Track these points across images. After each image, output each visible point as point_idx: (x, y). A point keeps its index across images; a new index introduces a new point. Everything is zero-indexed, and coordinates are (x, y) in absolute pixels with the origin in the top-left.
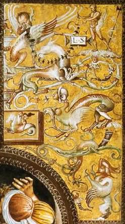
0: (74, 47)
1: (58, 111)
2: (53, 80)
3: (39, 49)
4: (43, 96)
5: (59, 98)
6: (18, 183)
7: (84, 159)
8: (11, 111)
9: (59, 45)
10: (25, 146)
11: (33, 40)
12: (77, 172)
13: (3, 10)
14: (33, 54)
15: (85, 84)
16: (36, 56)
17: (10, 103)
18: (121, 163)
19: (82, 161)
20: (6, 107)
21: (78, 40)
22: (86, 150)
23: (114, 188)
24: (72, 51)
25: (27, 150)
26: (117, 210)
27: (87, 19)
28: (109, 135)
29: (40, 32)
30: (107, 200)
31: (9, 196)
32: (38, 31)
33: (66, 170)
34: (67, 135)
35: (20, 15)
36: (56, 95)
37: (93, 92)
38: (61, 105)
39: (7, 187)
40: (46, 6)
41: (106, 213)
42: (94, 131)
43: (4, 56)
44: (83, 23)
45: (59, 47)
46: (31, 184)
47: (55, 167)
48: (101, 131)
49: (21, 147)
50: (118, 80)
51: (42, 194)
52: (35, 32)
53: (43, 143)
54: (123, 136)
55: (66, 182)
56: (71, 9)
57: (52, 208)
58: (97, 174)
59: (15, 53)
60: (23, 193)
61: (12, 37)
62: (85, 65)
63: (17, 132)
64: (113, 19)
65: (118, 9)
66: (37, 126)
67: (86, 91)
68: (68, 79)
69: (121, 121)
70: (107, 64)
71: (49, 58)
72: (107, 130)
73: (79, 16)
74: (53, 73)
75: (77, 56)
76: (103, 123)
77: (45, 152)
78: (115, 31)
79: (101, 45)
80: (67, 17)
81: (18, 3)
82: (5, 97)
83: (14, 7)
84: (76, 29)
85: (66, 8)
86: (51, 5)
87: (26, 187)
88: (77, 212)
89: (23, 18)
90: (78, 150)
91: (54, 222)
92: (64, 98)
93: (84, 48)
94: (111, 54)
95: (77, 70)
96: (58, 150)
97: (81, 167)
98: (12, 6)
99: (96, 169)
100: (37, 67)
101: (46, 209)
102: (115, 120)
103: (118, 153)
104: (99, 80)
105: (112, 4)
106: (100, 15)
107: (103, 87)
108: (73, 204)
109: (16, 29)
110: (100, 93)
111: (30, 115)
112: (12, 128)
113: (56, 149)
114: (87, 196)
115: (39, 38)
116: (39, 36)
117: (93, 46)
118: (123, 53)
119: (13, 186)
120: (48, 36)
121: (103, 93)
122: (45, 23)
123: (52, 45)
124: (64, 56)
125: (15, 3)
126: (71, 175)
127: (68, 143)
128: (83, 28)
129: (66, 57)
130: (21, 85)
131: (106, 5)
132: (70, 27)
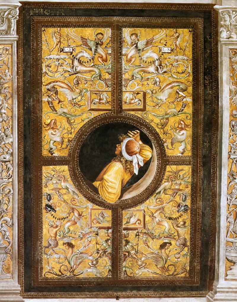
1: (154, 91)
2: (152, 73)
3: (143, 55)
4: (145, 83)
5: (155, 84)
6: (131, 134)
7: (169, 119)
8: (127, 92)
9: (155, 53)
10: (135, 112)
11: (140, 50)
12: (165, 127)
13: (122, 32)
14: (140, 58)
15: (171, 75)
16: (141, 59)
17: (126, 87)
18: (191, 122)
19: (168, 121)
20: (124, 89)
21: (166, 50)
22: (171, 114)
23: (187, 136)
24: (162, 56)
25: (136, 114)
26: (189, 149)
27: (172, 38)
28: (185, 105)
29: (144, 45)
30: (183, 144)
32: (143, 44)
33: (159, 126)
34: (159, 105)
35: (132, 35)
36: (153, 82)
37: (175, 80)
38: (156, 88)
39: (125, 136)
40: (148, 30)
41: (183, 151)
42: (175, 103)
43: (123, 59)
44: (169, 40)
45: (154, 53)
46: (139, 134)
47: (153, 124)
48: (180, 103)
49: (132, 113)
50: (190, 73)
51: (145, 140)
52: (141, 45)
53: (145, 110)
54: (193, 106)
55: (159, 133)
56: (162, 31)
58: (177, 128)
59: (129, 57)
61: (128, 48)
62: (170, 64)
63: (130, 103)
64: (187, 38)
65: (189, 31)
66: (142, 100)
67: (171, 79)
68: (160, 72)
69: (191, 97)
70: (183, 63)
71: (149, 60)
72: (183, 103)
73: (166, 35)
74: (152, 69)
75: (166, 59)
76: (181, 98)
77: (147, 116)
78: (188, 44)
79: (180, 53)
80: (160, 36)
81: (131, 28)
82: (123, 83)
83: (129, 30)
84: (165, 43)
85: (159, 31)
86: (150, 29)
87: (136, 136)
88: (165, 150)
89: (134, 37)
90: (166, 114)
91: (152, 156)
92: (158, 84)
93: (170, 54)
94: (186, 58)
95: (165, 67)
96: (154, 114)
98: (127, 29)
99: (177, 125)
100: (142, 66)
101: (148, 149)
102: (188, 96)
103: (190, 116)
104: (179, 73)
105: (186, 28)
106: (179, 35)
107: (181, 77)
108: (163, 146)
109: (130, 43)
110: (179, 80)
111: (138, 94)
112: (128, 101)
113: (153, 114)
115: (143, 48)
116: (144, 47)
117: (175, 53)
118: (193, 57)
119: (128, 135)
120: (148, 47)
121: (181, 81)
122: (147, 40)
123: (150, 53)
124: (158, 59)
125: (129, 28)
126: (162, 129)
127: (160, 110)
128: (169, 43)
129: (159, 59)
130: (133, 76)
131: (183, 29)
132: (161, 42)
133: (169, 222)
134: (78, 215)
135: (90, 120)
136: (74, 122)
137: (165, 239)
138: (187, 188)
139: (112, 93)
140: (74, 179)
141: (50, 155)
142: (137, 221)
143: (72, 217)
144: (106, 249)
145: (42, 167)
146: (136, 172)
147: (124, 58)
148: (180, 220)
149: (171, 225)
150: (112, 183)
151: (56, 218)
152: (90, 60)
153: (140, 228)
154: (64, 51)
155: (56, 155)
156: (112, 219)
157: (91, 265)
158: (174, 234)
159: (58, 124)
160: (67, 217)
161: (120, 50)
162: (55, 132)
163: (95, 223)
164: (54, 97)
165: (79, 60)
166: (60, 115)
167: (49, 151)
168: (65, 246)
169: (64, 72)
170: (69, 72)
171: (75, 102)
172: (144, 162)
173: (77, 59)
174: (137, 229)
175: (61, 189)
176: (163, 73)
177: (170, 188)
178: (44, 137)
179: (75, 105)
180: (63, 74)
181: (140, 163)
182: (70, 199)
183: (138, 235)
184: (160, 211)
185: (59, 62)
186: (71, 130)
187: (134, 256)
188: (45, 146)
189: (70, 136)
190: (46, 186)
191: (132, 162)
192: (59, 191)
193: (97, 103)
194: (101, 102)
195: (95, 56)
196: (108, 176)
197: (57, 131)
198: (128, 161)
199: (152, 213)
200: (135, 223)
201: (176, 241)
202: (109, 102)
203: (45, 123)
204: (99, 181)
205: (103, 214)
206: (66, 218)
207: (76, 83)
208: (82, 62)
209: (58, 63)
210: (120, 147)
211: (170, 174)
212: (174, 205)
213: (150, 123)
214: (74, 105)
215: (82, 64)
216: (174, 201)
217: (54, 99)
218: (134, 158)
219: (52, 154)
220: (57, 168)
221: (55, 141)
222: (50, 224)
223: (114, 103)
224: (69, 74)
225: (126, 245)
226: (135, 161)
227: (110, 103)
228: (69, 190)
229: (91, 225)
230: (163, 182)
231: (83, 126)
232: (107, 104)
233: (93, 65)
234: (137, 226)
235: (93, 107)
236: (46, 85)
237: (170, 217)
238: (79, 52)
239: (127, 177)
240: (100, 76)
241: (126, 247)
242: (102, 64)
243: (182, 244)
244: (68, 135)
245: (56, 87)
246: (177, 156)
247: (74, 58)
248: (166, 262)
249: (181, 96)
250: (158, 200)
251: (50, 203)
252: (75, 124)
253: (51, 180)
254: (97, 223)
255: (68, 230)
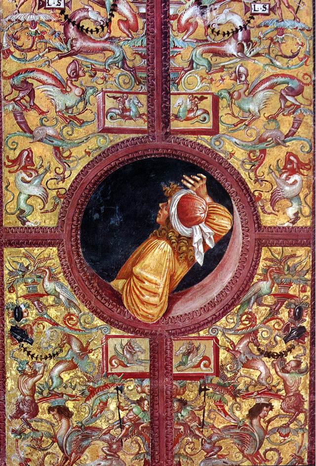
0: (255, 17)
1: (236, 94)
4: (217, 76)
5: (237, 78)
6: (188, 181)
7: (267, 152)
8: (179, 94)
10: (196, 136)
12: (259, 168)
15: (268, 61)
17: (178, 84)
20: (173, 90)
22: (269, 141)
24: (252, 21)
25: (199, 141)
26: (307, 214)
31: (177, 197)
33: (247, 165)
37: (278, 71)
39: (175, 186)
41: (294, 217)
45: (237, 15)
46: (205, 182)
49: (192, 138)
51: (218, 194)
53: (218, 133)
55: (247, 180)
57: (231, 213)
58: (284, 171)
59: (183, 21)
60: (195, 193)
63: (188, 119)
68: (248, 55)
74: (231, 48)
76: (290, 109)
77: (220, 143)
82: (172, 76)
87: (198, 186)
88: (259, 216)
91: (232, 228)
92: (243, 79)
96: (237, 141)
97: (264, 162)
99: (282, 164)
104: (286, 57)
110: (286, 72)
111: (202, 99)
112: (181, 114)
113: (234, 140)
114: (271, 197)
119: (182, 184)
124: (242, 26)
126: (252, 171)
129: (246, 29)
130: (192, 62)
133: (267, 362)
134: (80, 350)
135: (104, 153)
136: (69, 157)
137: (259, 396)
138: (305, 291)
139: (149, 97)
140: (71, 275)
141: (20, 224)
142: (201, 361)
143: (67, 354)
144: (139, 419)
145: (3, 250)
146: (200, 260)
147: (174, 23)
148: (290, 358)
149: (271, 367)
150: (150, 282)
151: (32, 356)
152: (102, 27)
153: (207, 375)
154: (47, 6)
155: (33, 225)
156: (150, 357)
157: (108, 452)
158: (277, 387)
159: (37, 161)
160: (57, 354)
161: (164, 7)
162: (30, 175)
163: (116, 365)
164: (27, 102)
165: (78, 25)
166: (39, 141)
167: (18, 217)
168: (53, 415)
169: (47, 50)
170: (59, 50)
171: (72, 113)
172: (215, 240)
173: (74, 24)
174: (203, 378)
175: (44, 295)
176: (253, 56)
177: (269, 291)
178: (7, 187)
179: (70, 121)
180: (45, 55)
181: (208, 242)
182: (64, 315)
183: (205, 389)
184: (248, 340)
185: (36, 29)
186: (63, 173)
187: (197, 432)
188: (8, 206)
189: (61, 185)
190: (12, 289)
191: (190, 239)
192: (38, 301)
193: (118, 117)
194: (126, 116)
195: (113, 19)
196: (142, 269)
197: (34, 175)
198: (182, 238)
199: (233, 343)
200: (198, 366)
201: (281, 401)
202: (144, 114)
203: (8, 157)
204: (123, 279)
205: (131, 346)
206: (54, 355)
207: (73, 74)
208: (84, 31)
209: (34, 30)
210: (166, 210)
211: (269, 263)
212: (276, 326)
213: (228, 159)
214: (68, 121)
215: (86, 35)
216: (278, 320)
217: (26, 107)
218: (196, 231)
219: (24, 223)
220: (36, 251)
221: (30, 196)
222: (20, 369)
223: (154, 116)
224: (58, 55)
225: (179, 411)
226: (197, 237)
227: (144, 117)
228: (61, 297)
229: (107, 370)
230: (255, 280)
231: (88, 164)
232: (141, 121)
233: (109, 38)
234: (202, 370)
235: (109, 124)
236: (9, 78)
237: (269, 351)
238: (80, 9)
239: (182, 271)
240: (124, 60)
241: (179, 414)
242: (128, 36)
243: (294, 407)
244: (58, 184)
245: (30, 81)
246: (283, 227)
247: (70, 21)
248: (261, 443)
249: (291, 106)
250: (244, 317)
251: (21, 324)
252: (71, 159)
253: (23, 276)
254: (120, 365)
255: (59, 380)
